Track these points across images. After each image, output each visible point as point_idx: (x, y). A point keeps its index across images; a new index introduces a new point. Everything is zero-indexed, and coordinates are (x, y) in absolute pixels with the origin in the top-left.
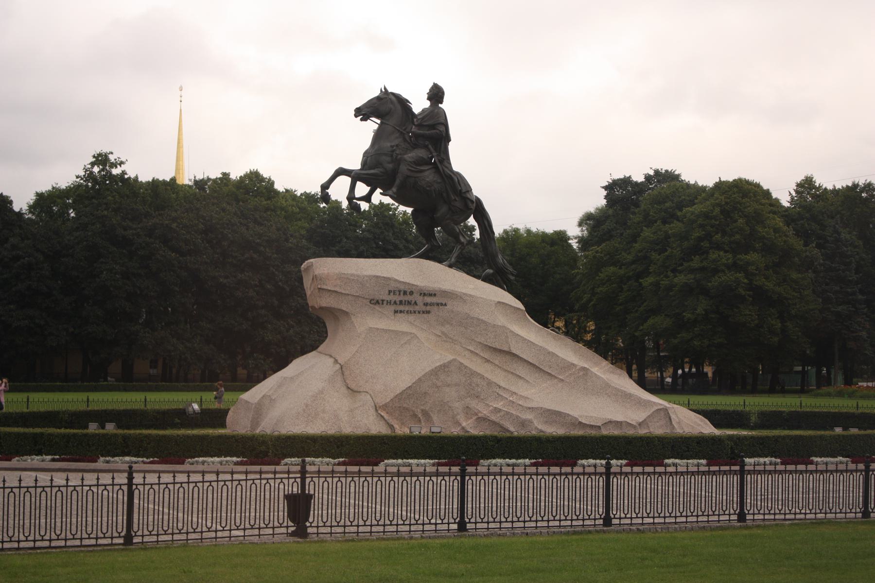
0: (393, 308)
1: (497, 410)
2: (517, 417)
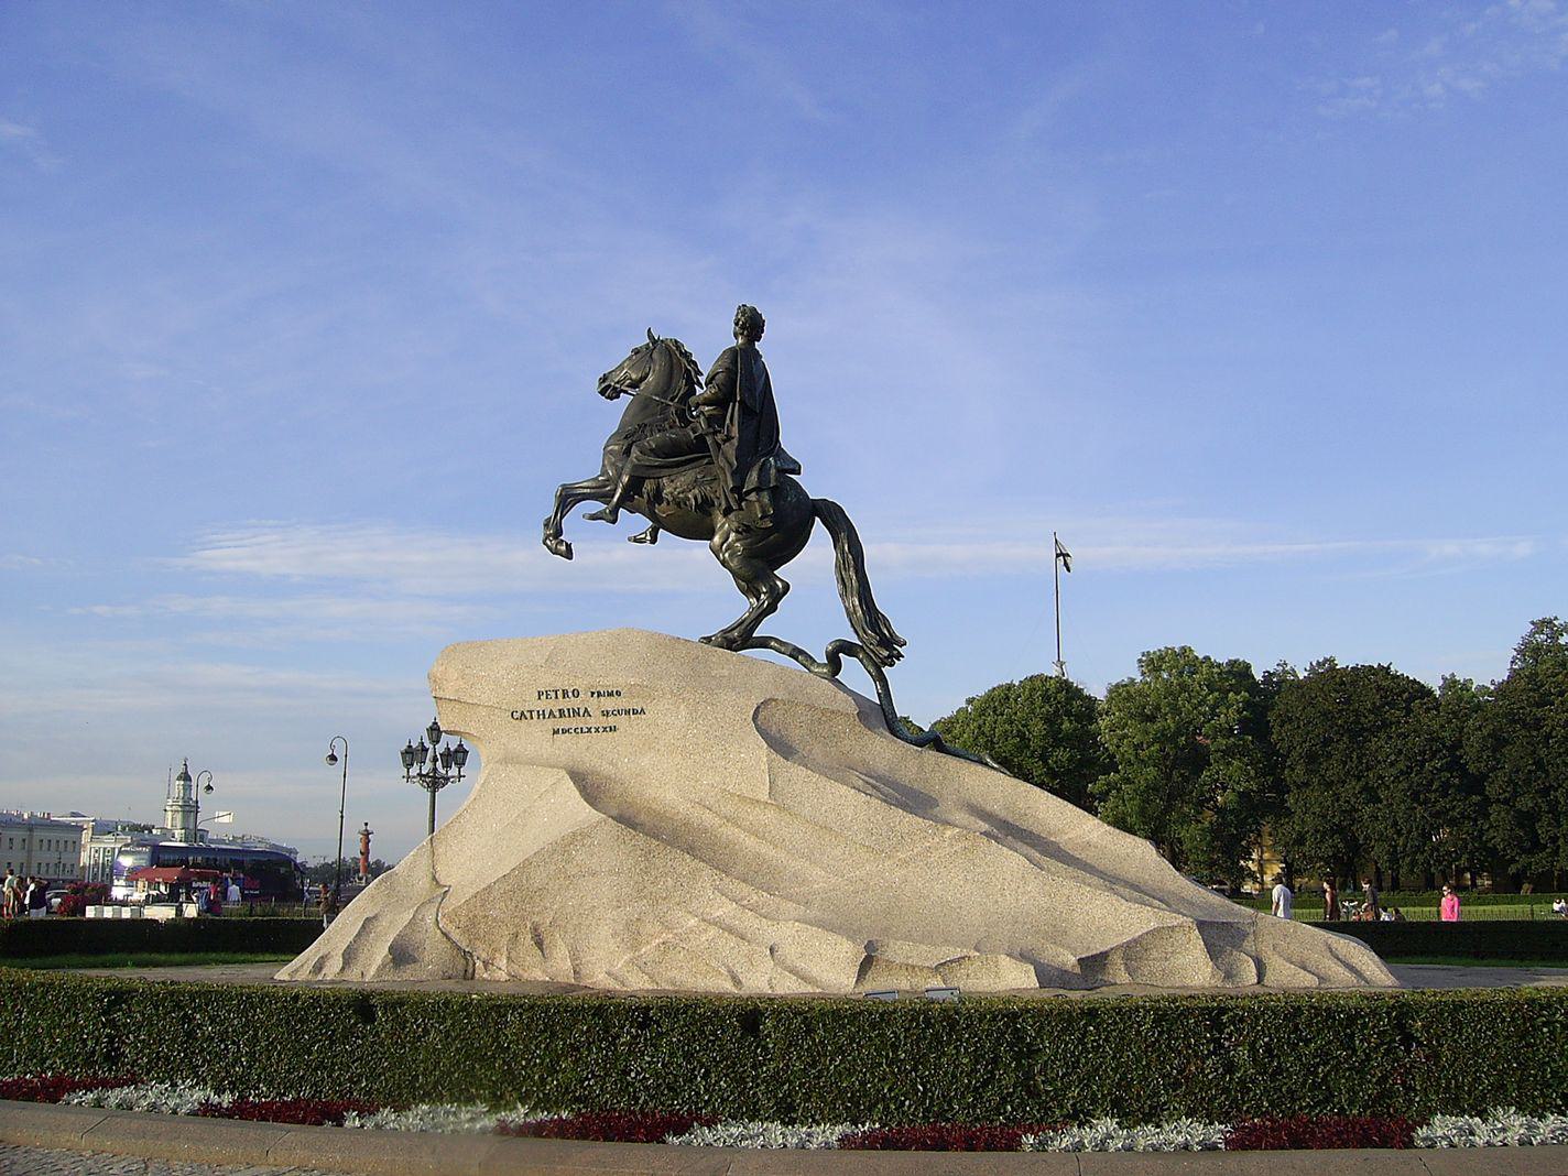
0: (550, 724)
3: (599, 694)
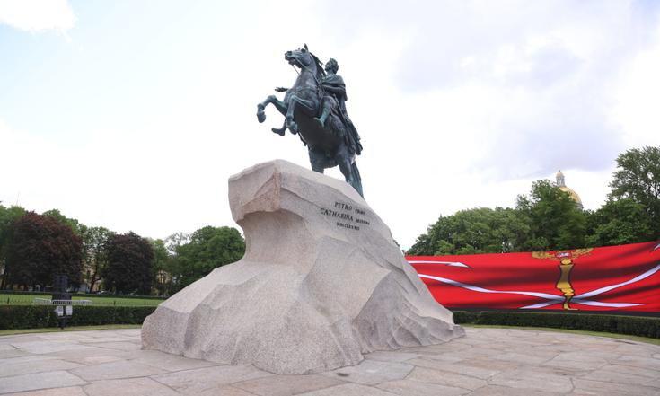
1: (408, 320)
2: (420, 326)
3: (358, 211)
